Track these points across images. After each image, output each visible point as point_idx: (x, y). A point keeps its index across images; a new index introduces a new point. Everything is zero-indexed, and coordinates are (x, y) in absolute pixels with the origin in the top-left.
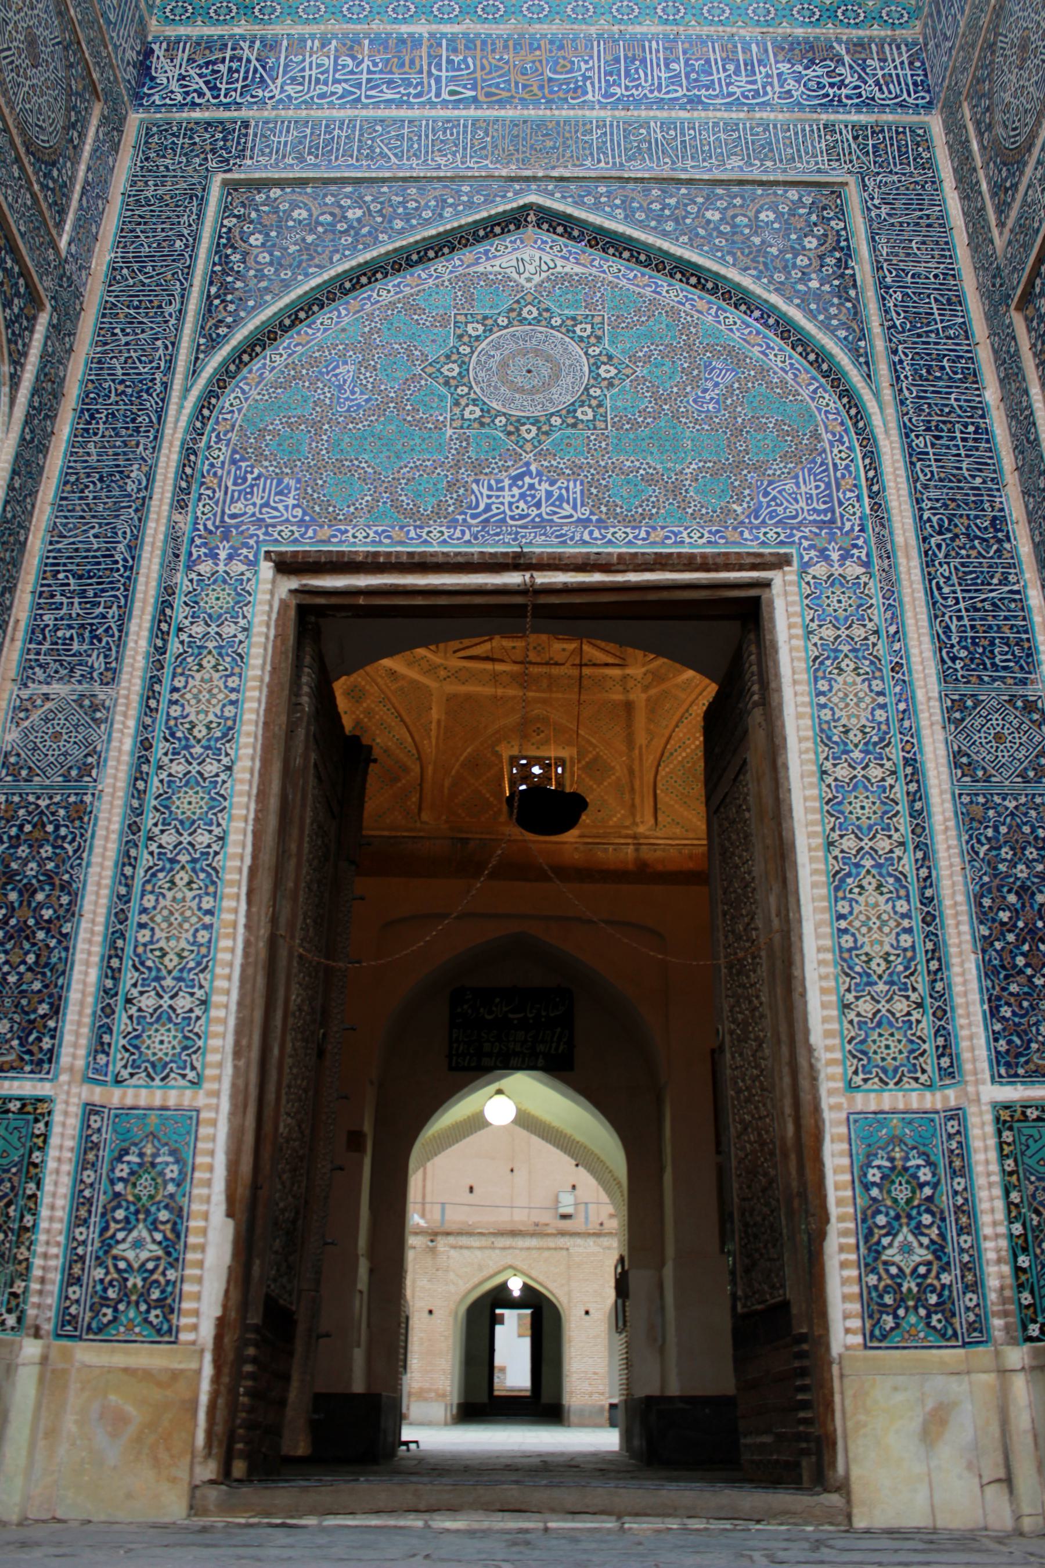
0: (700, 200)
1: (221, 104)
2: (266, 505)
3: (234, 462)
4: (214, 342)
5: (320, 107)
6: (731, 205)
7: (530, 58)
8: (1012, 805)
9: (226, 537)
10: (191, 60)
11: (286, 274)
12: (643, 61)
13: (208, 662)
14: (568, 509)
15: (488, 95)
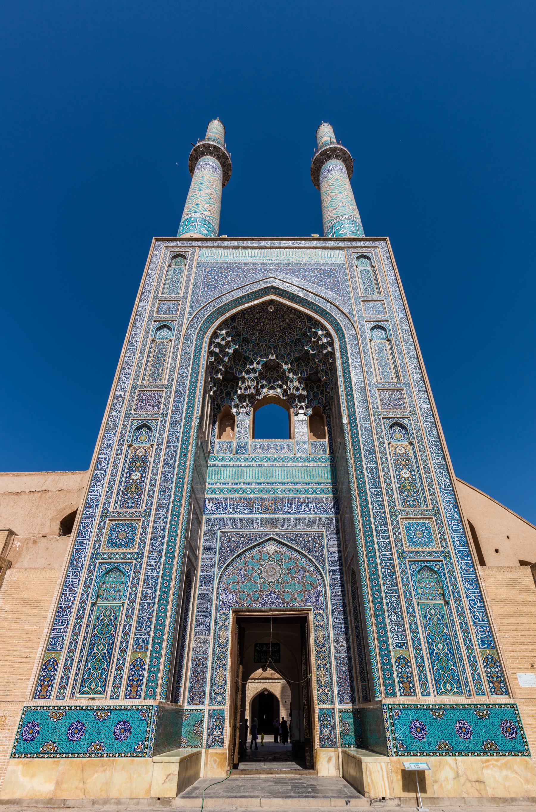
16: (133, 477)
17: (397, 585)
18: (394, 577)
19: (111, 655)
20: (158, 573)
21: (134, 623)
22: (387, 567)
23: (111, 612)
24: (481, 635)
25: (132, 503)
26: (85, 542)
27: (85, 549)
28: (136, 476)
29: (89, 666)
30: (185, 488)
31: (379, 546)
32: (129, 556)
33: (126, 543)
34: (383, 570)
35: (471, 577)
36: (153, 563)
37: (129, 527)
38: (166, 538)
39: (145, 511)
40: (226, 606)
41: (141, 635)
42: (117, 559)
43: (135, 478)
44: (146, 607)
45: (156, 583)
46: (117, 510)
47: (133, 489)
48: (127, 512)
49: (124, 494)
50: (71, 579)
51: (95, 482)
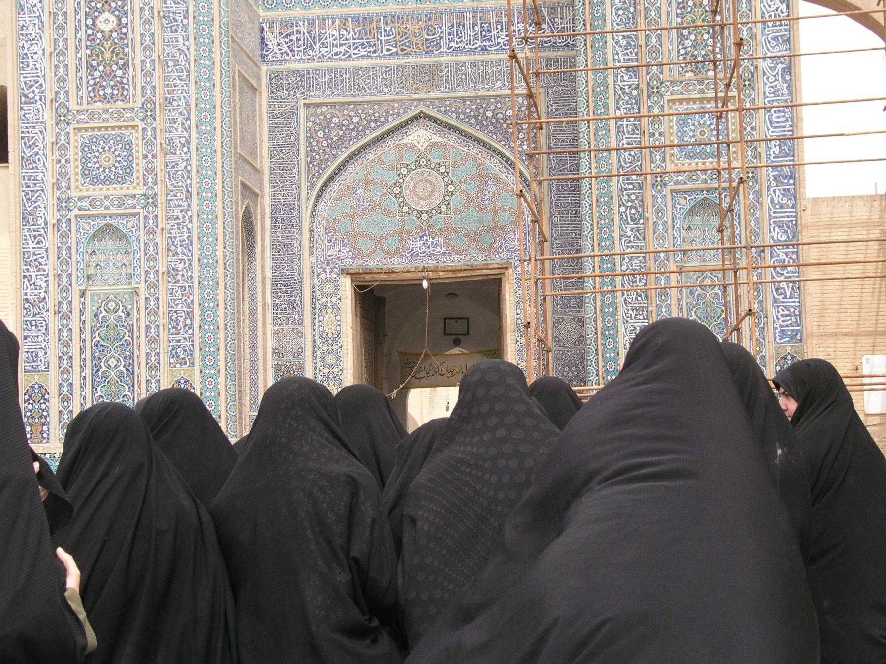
0: (485, 106)
1: (296, 60)
2: (340, 251)
3: (326, 233)
4: (312, 186)
5: (336, 60)
6: (496, 108)
7: (418, 27)
8: (569, 353)
9: (328, 264)
10: (281, 34)
11: (334, 152)
12: (463, 26)
13: (329, 311)
14: (439, 249)
15: (402, 50)
16: (101, 25)
17: (644, 238)
18: (642, 221)
19: (133, 374)
20: (190, 231)
21: (162, 320)
22: (629, 204)
23: (117, 304)
24: (783, 321)
25: (113, 89)
26: (39, 177)
27: (43, 191)
28: (107, 22)
29: (100, 393)
30: (217, 44)
31: (619, 161)
32: (130, 202)
33: (117, 175)
34: (622, 209)
35: (788, 217)
36: (177, 213)
37: (117, 143)
38: (194, 163)
39: (142, 107)
40: (332, 265)
41: (179, 341)
42: (107, 208)
43: (107, 28)
44: (179, 294)
45: (190, 251)
46: (85, 106)
47: (108, 55)
48: (107, 111)
49: (90, 66)
50: (32, 251)
51: (27, 45)
